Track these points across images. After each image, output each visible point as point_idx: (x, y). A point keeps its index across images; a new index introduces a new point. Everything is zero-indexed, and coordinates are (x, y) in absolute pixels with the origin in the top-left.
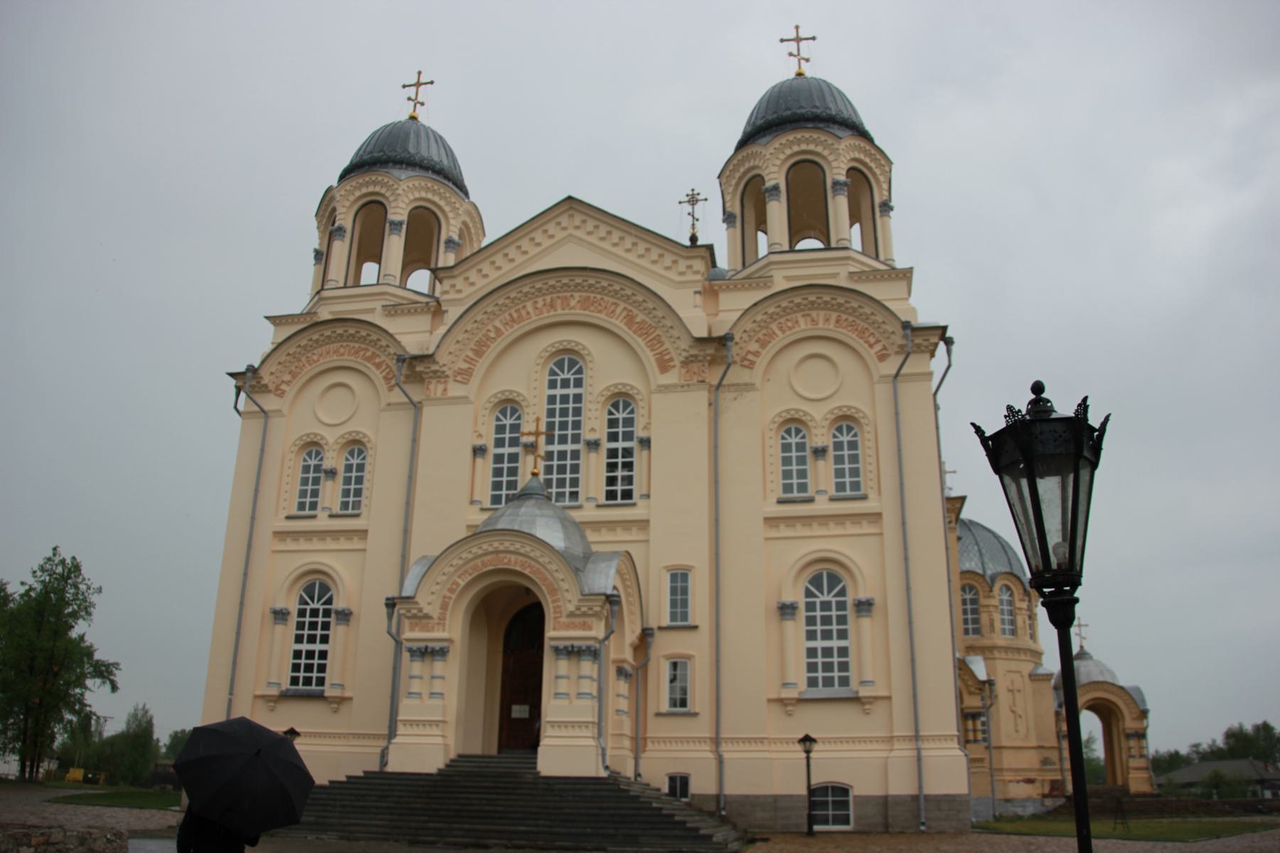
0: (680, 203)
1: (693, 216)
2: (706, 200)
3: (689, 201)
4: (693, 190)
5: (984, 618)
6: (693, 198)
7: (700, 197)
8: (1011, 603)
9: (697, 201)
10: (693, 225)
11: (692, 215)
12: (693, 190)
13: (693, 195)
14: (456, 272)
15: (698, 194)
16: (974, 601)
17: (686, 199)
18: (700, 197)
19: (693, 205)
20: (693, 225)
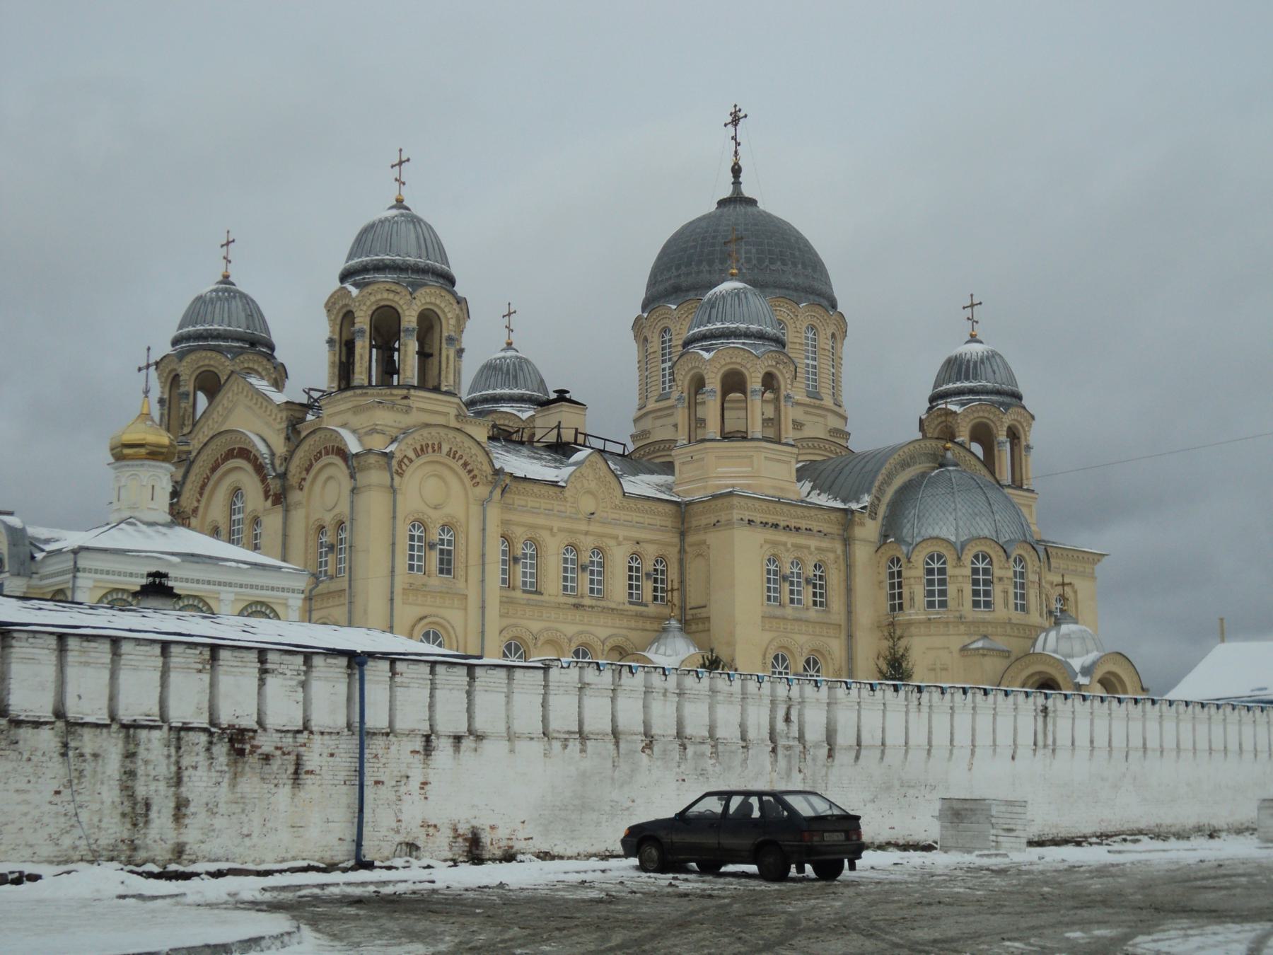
0: (726, 125)
1: (736, 140)
2: (746, 116)
3: (733, 121)
4: (735, 106)
5: (905, 591)
6: (735, 116)
7: (741, 114)
8: (942, 571)
9: (739, 119)
10: (736, 152)
11: (734, 138)
12: (735, 106)
13: (736, 112)
14: (195, 433)
15: (740, 110)
16: (899, 573)
17: (730, 119)
18: (741, 114)
19: (736, 125)
20: (736, 152)
